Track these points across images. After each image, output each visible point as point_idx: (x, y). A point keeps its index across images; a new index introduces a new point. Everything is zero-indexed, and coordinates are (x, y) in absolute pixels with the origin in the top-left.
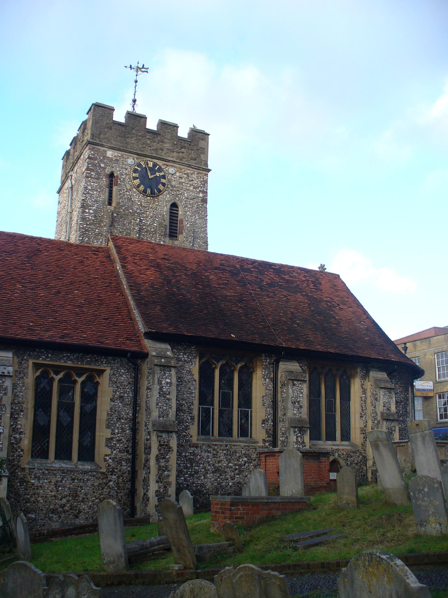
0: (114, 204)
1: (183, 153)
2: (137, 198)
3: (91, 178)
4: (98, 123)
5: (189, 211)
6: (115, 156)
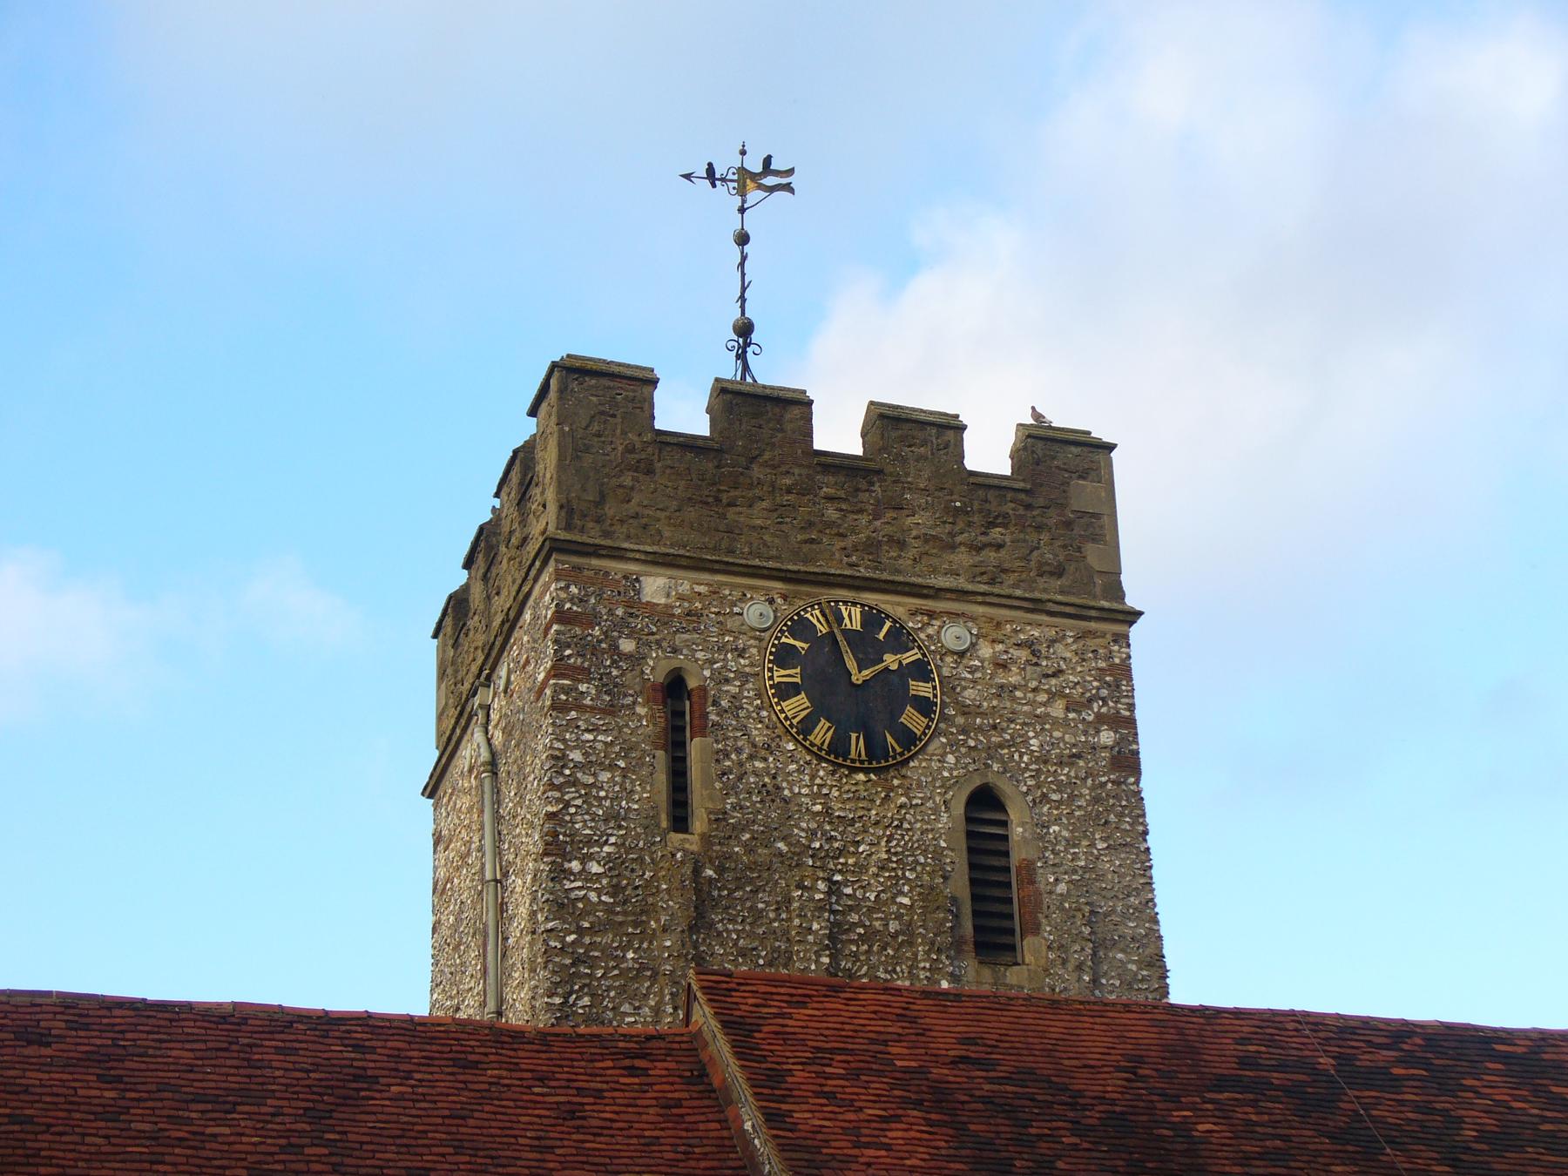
0: (699, 824)
1: (999, 547)
2: (806, 782)
3: (580, 708)
4: (587, 449)
5: (1057, 820)
6: (681, 598)
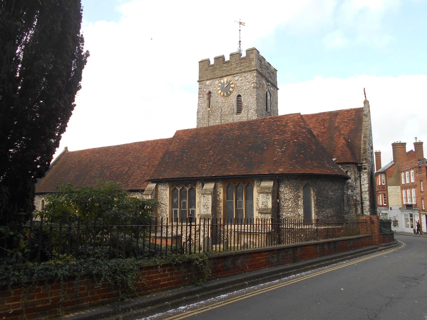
2: (221, 99)
